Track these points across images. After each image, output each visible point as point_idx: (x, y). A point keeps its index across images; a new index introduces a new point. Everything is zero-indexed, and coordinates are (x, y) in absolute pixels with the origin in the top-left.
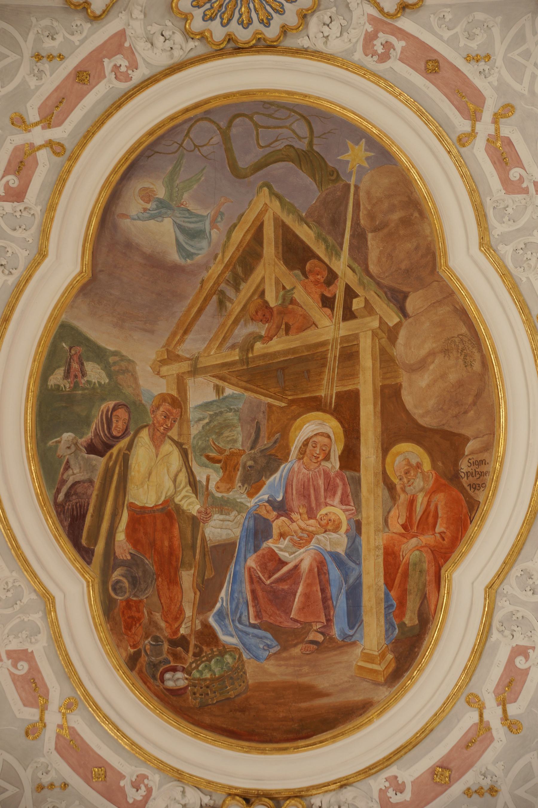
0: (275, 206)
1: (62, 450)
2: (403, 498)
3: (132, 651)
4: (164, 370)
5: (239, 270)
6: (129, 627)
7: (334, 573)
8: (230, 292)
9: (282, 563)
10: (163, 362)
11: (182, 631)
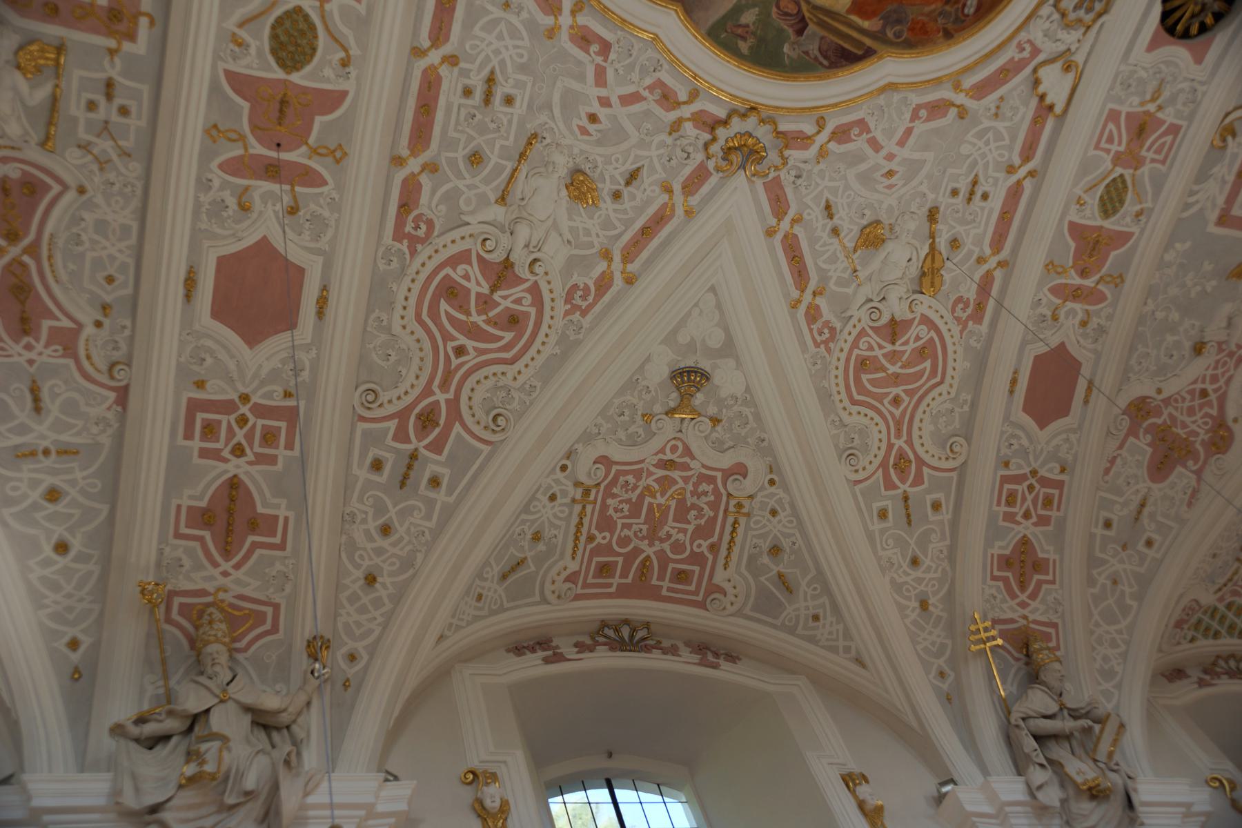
1: (794, 55)
3: (941, 34)
6: (926, 33)
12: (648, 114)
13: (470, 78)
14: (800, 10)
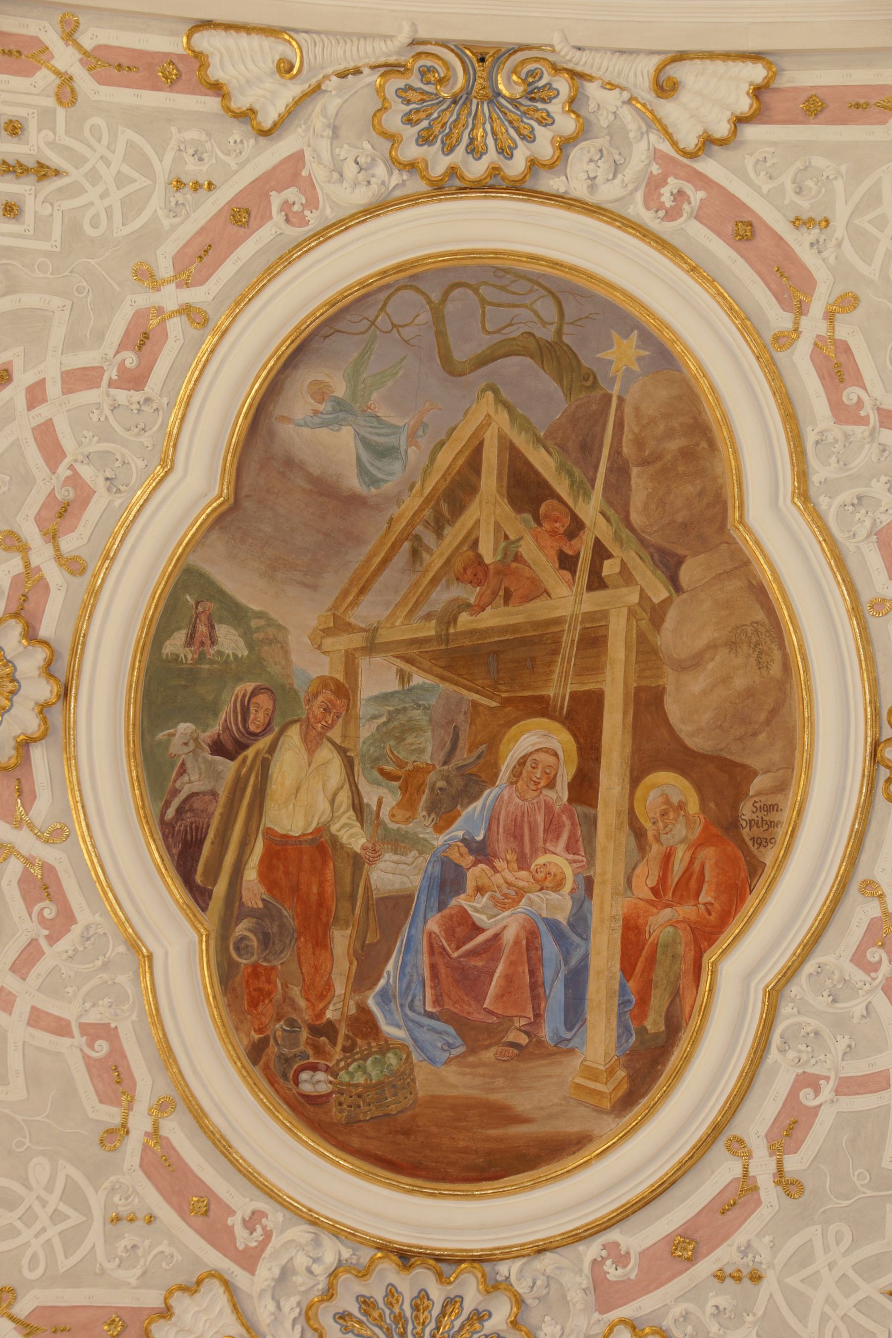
0: (502, 419)
1: (175, 746)
2: (655, 850)
3: (257, 1037)
4: (328, 643)
5: (444, 507)
6: (254, 1003)
7: (550, 948)
8: (429, 538)
9: (479, 930)
10: (327, 632)
11: (329, 1015)
12: (28, 481)
13: (39, 131)
14: (256, 736)
